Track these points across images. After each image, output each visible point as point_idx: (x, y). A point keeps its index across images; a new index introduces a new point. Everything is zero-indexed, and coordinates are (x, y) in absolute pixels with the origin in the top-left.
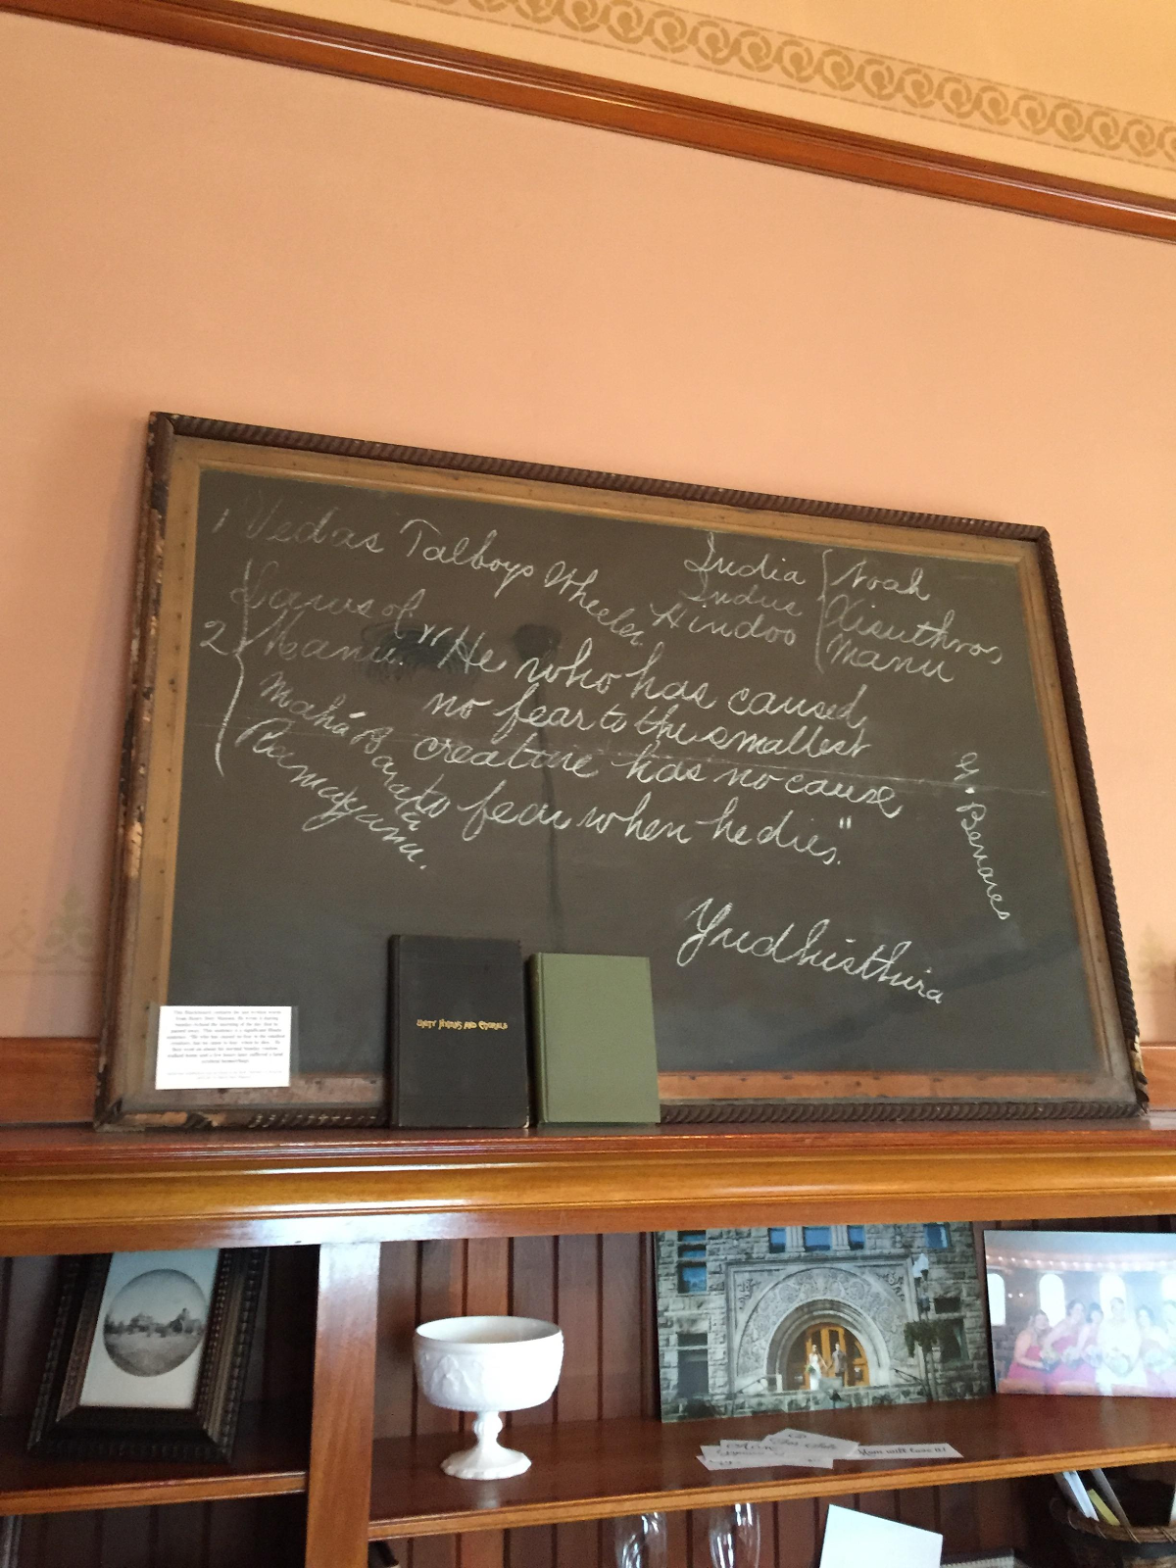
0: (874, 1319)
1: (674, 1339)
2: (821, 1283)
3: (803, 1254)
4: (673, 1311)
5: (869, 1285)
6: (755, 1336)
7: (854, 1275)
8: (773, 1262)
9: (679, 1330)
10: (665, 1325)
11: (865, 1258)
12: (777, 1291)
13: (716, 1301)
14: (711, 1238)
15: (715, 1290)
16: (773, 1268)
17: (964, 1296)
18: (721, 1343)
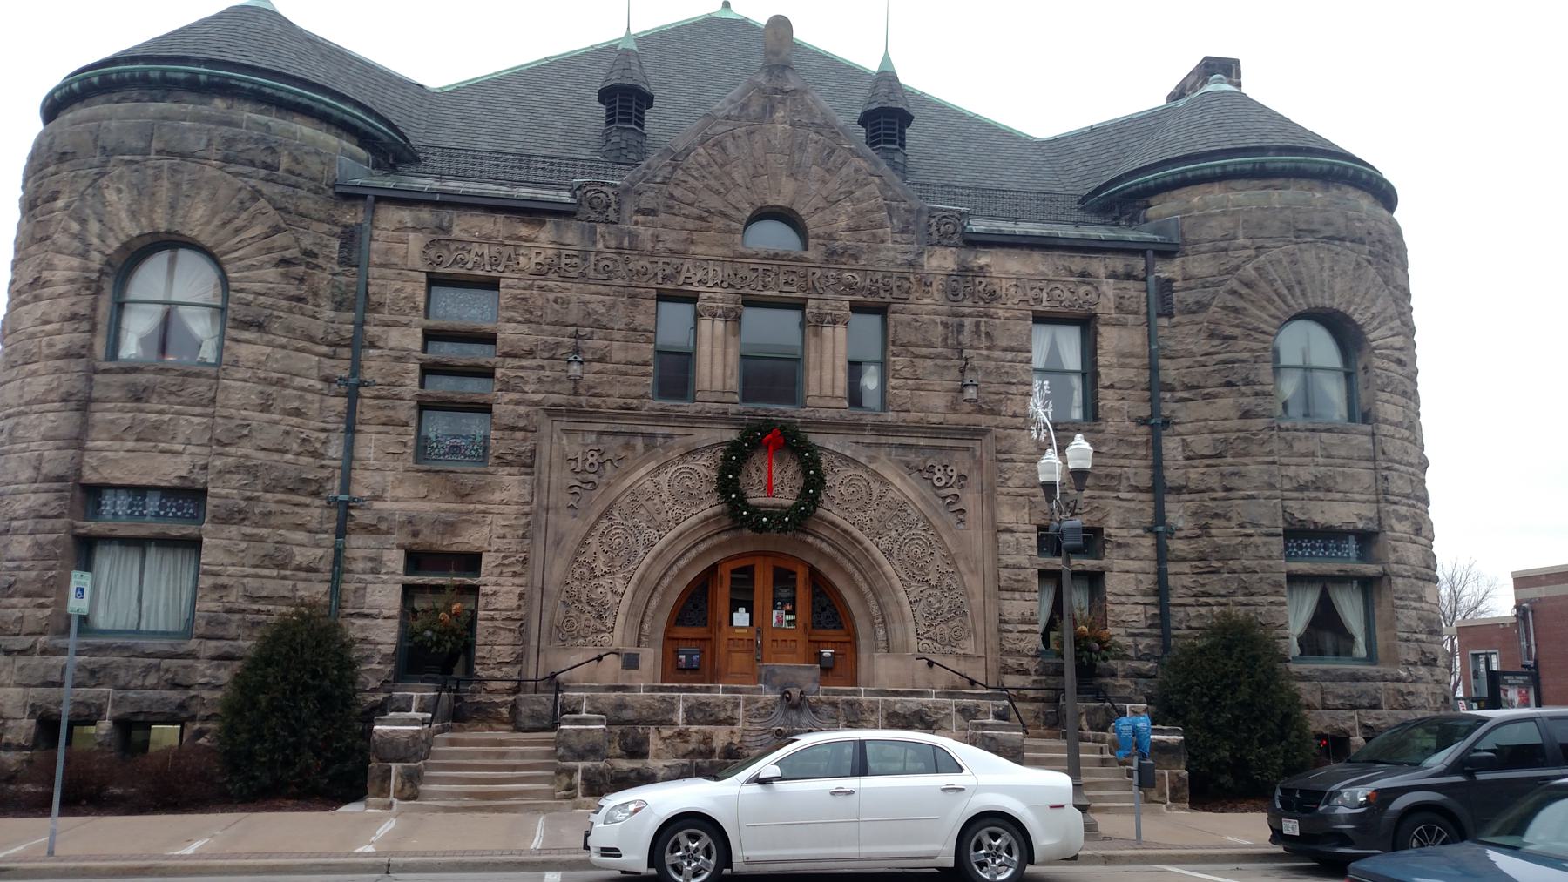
0: (888, 554)
1: (395, 560)
3: (732, 409)
4: (397, 500)
5: (886, 483)
6: (600, 567)
8: (662, 417)
9: (410, 540)
12: (664, 479)
13: (510, 487)
14: (505, 355)
15: (509, 464)
16: (659, 430)
17: (1111, 528)
18: (515, 574)
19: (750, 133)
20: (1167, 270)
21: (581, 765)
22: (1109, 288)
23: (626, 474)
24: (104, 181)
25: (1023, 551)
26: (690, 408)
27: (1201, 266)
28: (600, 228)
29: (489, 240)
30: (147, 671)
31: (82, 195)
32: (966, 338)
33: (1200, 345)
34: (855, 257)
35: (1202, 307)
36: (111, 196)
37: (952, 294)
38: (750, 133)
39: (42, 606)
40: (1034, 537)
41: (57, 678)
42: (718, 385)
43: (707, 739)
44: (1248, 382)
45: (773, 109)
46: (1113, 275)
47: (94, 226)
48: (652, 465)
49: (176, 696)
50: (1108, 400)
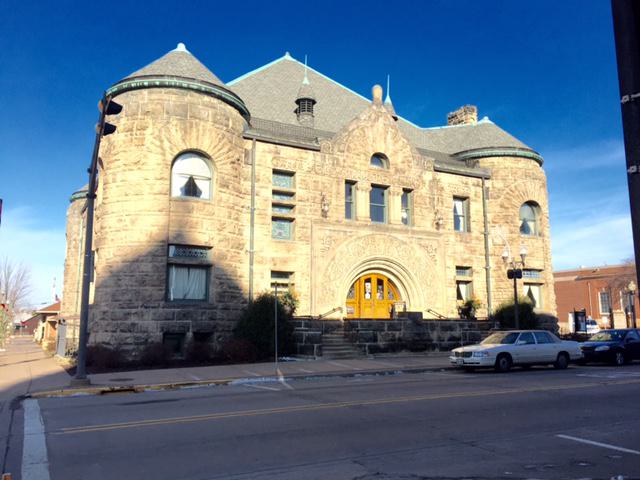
0: (416, 274)
2: (382, 246)
6: (332, 278)
7: (405, 243)
8: (349, 225)
10: (260, 262)
11: (414, 232)
13: (303, 249)
19: (372, 126)
20: (488, 183)
21: (367, 344)
22: (473, 188)
23: (339, 245)
24: (170, 126)
25: (452, 274)
26: (358, 223)
27: (499, 184)
28: (327, 156)
29: (292, 158)
30: (205, 313)
31: (160, 131)
32: (436, 203)
33: (498, 209)
34: (404, 173)
35: (499, 197)
36: (173, 131)
37: (431, 187)
38: (372, 126)
39: (161, 290)
40: (455, 270)
41: (171, 317)
42: (364, 215)
43: (394, 336)
44: (512, 222)
45: (376, 120)
46: (474, 185)
47: (166, 144)
48: (346, 243)
49: (212, 322)
50: (473, 225)
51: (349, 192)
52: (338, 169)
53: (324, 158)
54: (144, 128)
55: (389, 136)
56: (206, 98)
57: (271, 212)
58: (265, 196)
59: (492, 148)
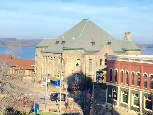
45: (106, 48)
51: (101, 61)
52: (99, 58)
53: (97, 56)
54: (71, 56)
55: (108, 50)
56: (80, 51)
57: (88, 66)
58: (88, 63)
59: (129, 49)
